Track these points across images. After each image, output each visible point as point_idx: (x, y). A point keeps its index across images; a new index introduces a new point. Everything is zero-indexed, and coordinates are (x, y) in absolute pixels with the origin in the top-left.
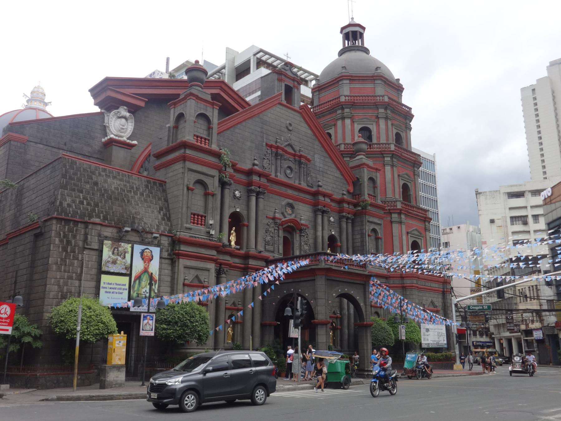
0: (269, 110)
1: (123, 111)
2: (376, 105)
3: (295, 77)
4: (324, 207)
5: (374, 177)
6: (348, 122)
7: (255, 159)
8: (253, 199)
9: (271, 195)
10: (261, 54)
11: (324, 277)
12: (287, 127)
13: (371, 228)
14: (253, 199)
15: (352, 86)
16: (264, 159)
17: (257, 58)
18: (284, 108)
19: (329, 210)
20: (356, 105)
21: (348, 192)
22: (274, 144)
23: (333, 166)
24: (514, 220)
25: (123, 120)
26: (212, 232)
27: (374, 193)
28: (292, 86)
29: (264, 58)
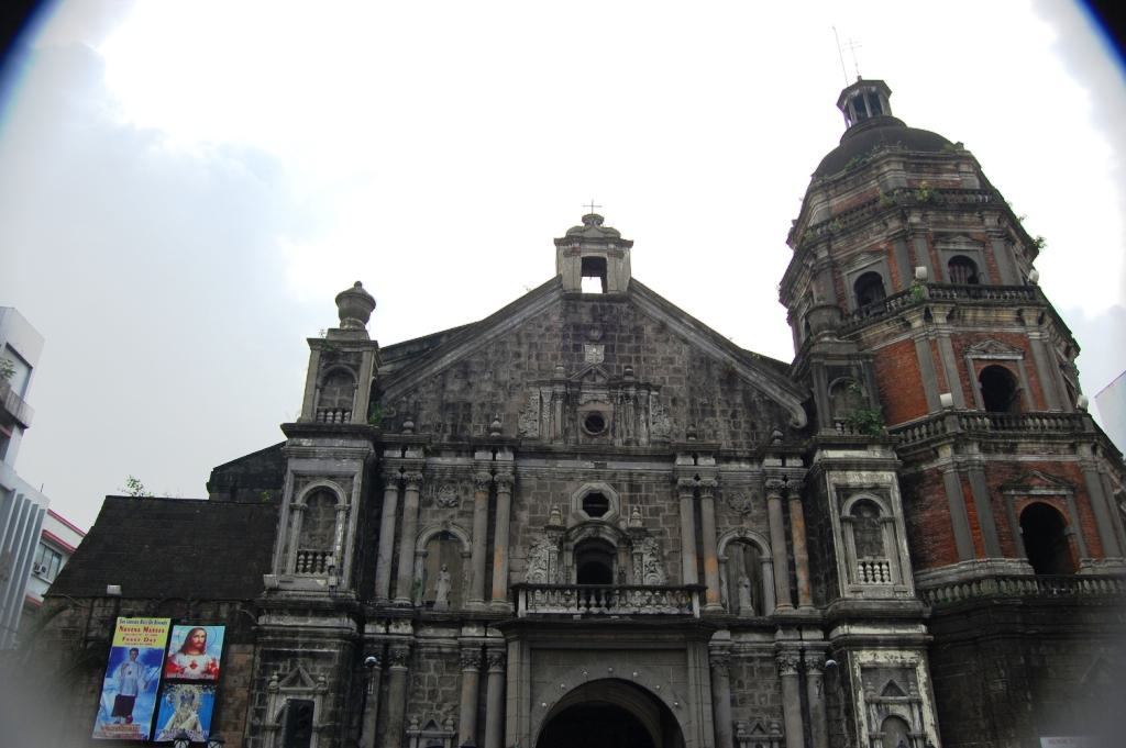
4: (697, 478)
28: (605, 255)
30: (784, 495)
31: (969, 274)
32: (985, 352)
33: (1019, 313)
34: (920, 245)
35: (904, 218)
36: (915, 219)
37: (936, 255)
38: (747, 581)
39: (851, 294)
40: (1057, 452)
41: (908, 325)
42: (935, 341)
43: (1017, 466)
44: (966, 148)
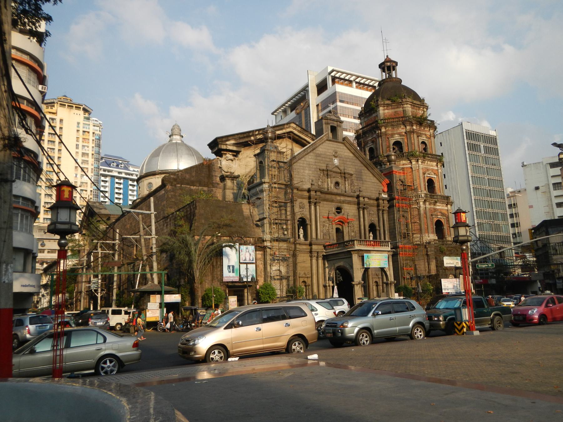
0: (320, 147)
1: (229, 156)
3: (338, 119)
4: (364, 205)
8: (313, 207)
9: (325, 203)
10: (334, 72)
11: (357, 255)
14: (313, 207)
17: (332, 76)
18: (331, 142)
22: (325, 168)
23: (371, 175)
24: (557, 186)
25: (230, 161)
26: (286, 233)
28: (335, 125)
29: (337, 75)
30: (383, 211)
31: (424, 147)
32: (429, 174)
33: (437, 163)
34: (415, 136)
35: (412, 126)
36: (414, 127)
37: (418, 140)
39: (392, 146)
40: (443, 206)
41: (411, 162)
42: (419, 169)
43: (435, 210)
44: (426, 102)
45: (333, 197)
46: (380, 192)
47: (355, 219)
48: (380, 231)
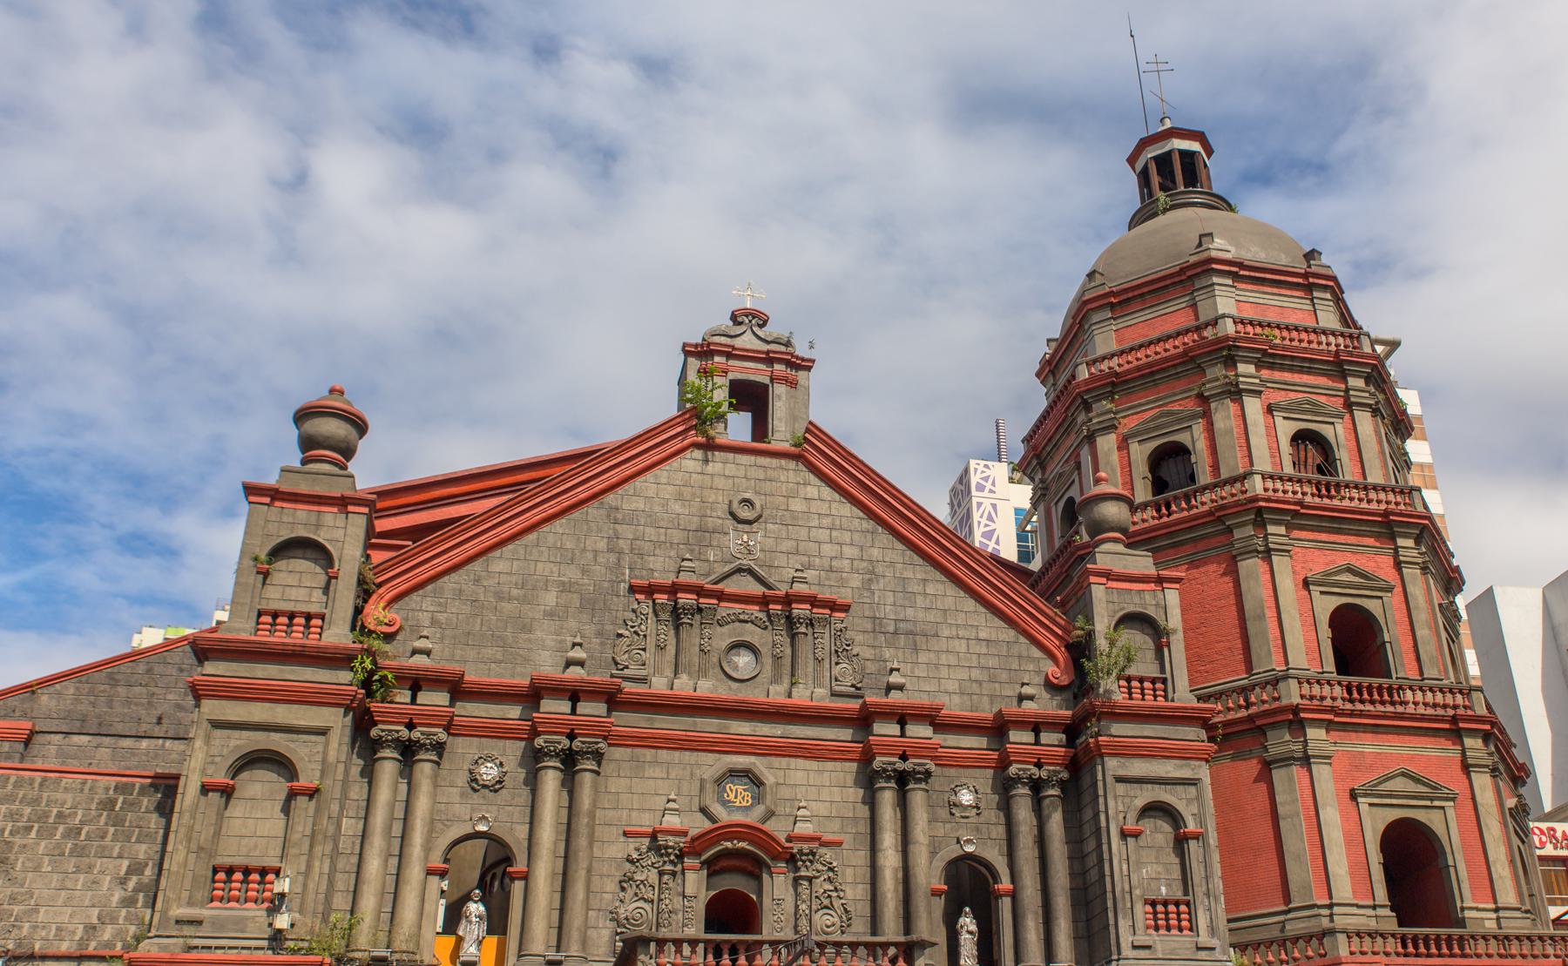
0: (649, 476)
2: (1192, 359)
4: (904, 757)
5: (1151, 612)
6: (1107, 444)
7: (574, 645)
12: (732, 514)
13: (1140, 803)
15: (1121, 323)
16: (620, 636)
19: (931, 765)
20: (1127, 381)
21: (1050, 686)
22: (669, 579)
27: (1163, 670)
28: (767, 381)
30: (1036, 786)
35: (1230, 362)
38: (973, 928)
39: (1141, 469)
45: (709, 726)
46: (1027, 690)
47: (847, 839)
48: (1014, 895)
